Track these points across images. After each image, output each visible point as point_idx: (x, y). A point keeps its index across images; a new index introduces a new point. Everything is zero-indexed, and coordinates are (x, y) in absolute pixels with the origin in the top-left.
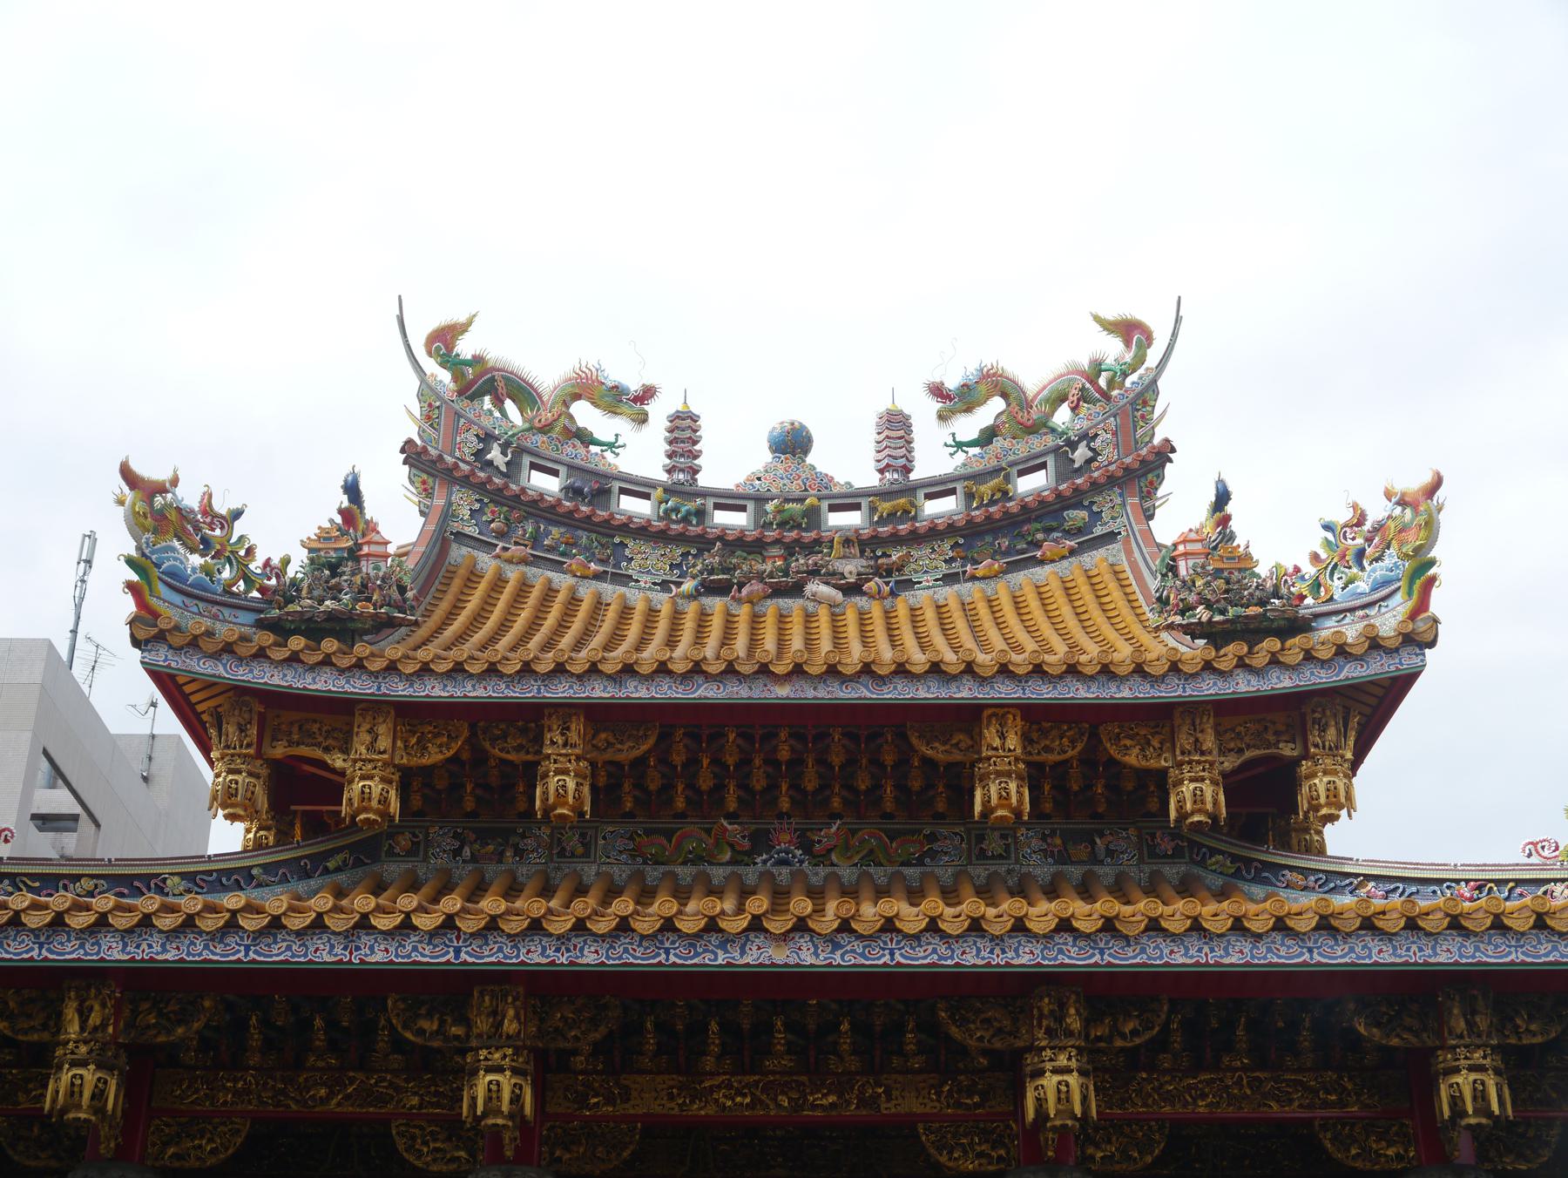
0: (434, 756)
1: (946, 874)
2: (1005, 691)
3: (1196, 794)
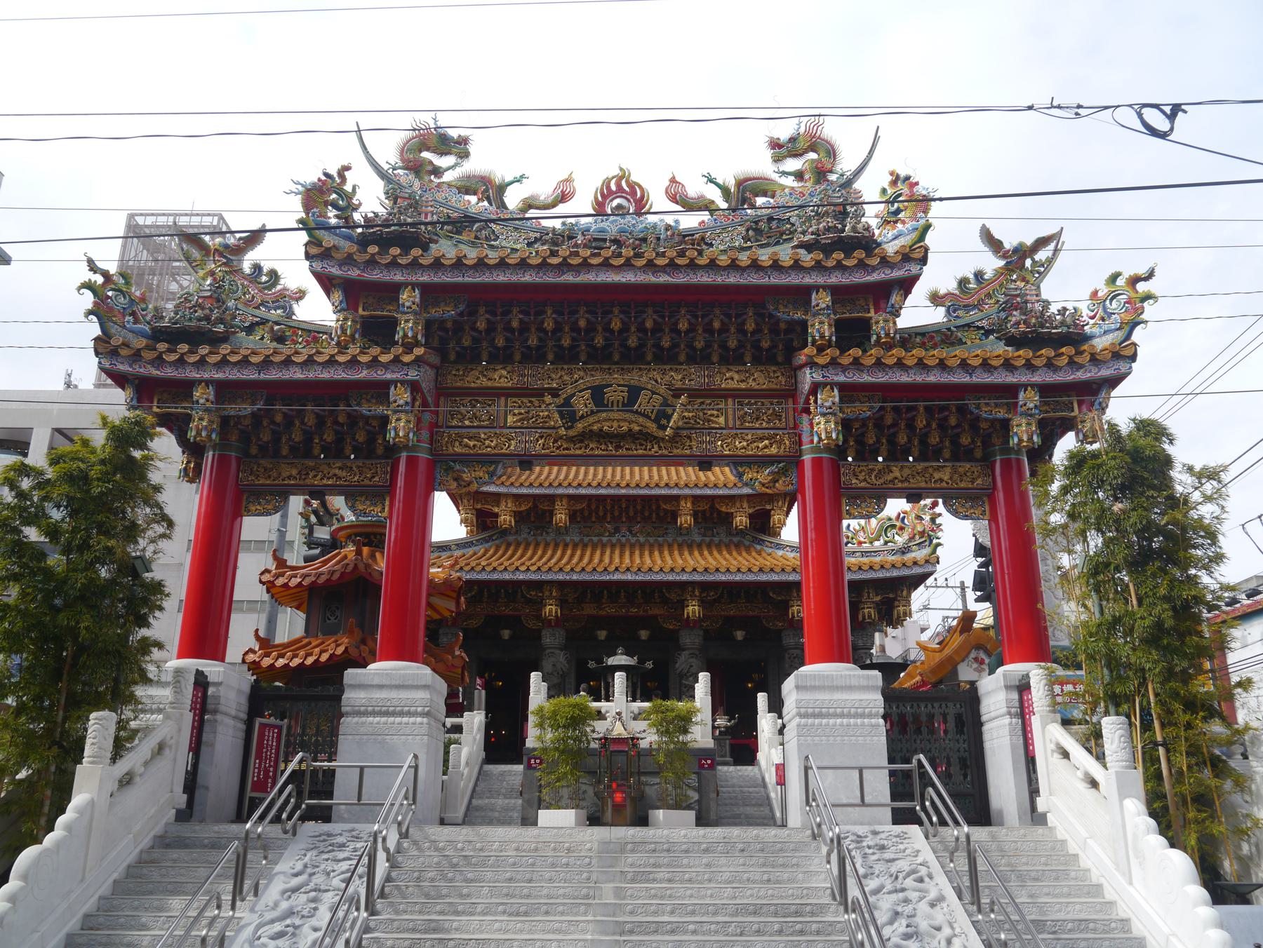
0: (523, 508)
1: (670, 540)
2: (687, 491)
3: (741, 520)
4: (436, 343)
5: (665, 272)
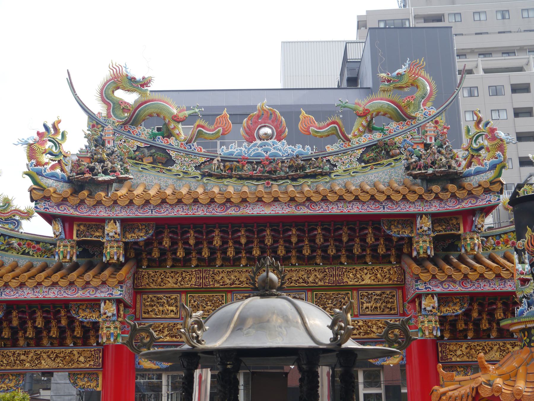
4: (133, 255)
5: (305, 205)
